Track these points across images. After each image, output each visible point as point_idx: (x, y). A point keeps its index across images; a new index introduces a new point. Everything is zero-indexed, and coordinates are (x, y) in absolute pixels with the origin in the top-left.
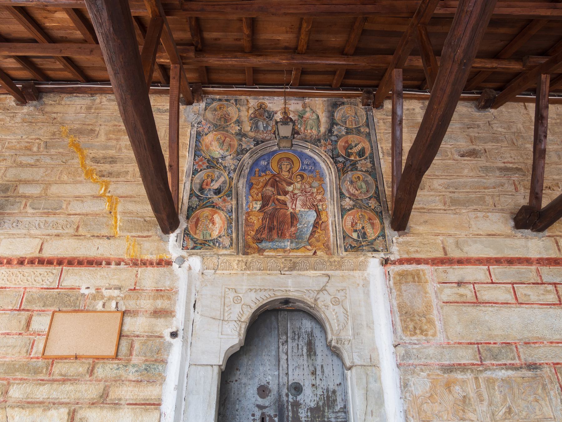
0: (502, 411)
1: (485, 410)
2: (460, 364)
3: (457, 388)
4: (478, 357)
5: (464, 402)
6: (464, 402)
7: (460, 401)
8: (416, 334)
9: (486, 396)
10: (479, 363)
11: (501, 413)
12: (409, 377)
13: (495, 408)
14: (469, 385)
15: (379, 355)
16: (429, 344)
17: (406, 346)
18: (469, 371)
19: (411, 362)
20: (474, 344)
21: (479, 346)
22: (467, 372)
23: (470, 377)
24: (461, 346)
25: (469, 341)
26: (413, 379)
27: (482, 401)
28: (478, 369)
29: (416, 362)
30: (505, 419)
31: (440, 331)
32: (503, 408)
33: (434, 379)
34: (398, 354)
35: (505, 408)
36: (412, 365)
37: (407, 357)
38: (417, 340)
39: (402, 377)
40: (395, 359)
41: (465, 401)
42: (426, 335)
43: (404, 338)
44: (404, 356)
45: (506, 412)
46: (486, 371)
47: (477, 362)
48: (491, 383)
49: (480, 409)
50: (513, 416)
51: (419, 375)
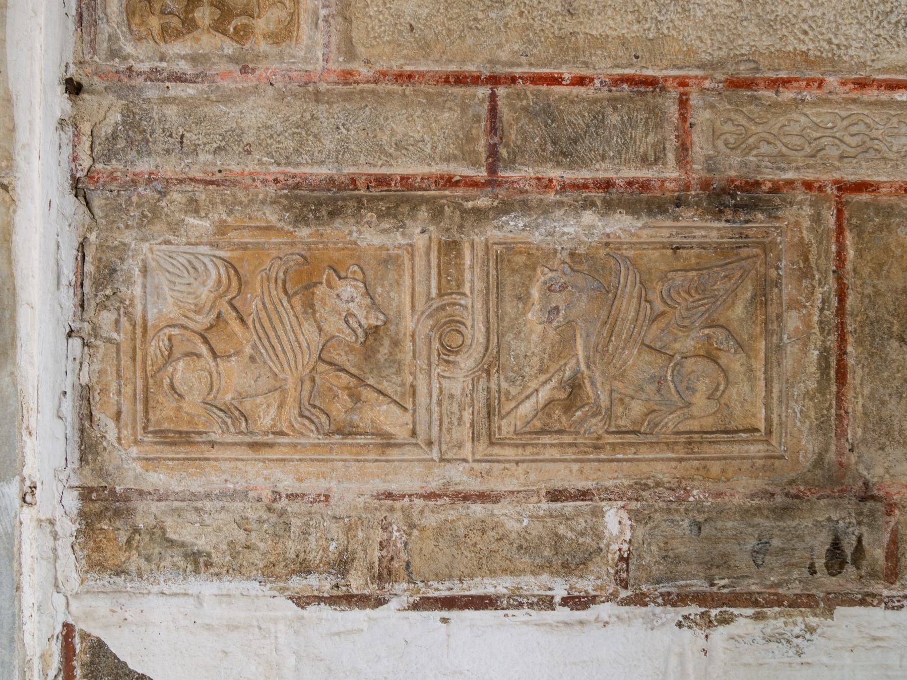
0: (533, 399)
1: (457, 392)
2: (383, 181)
3: (347, 289)
4: (481, 146)
5: (368, 351)
6: (368, 351)
7: (351, 349)
8: (190, 25)
9: (475, 332)
10: (482, 174)
11: (527, 408)
12: (128, 237)
13: (504, 385)
14: (407, 281)
15: (12, 130)
16: (251, 81)
17: (133, 88)
18: (423, 213)
19: (144, 166)
20: (476, 80)
21: (501, 91)
22: (413, 218)
23: (421, 241)
24: (409, 90)
25: (453, 68)
26: (145, 246)
27: (449, 352)
28: (470, 205)
29: (170, 167)
30: (542, 432)
31: (315, 13)
32: (544, 383)
33: (244, 247)
34: (86, 128)
35: (554, 382)
36: (149, 181)
37: (131, 142)
38: (194, 59)
39: (93, 237)
40: (67, 151)
41: (375, 351)
42: (242, 35)
43: (129, 49)
44: (114, 137)
45: (550, 403)
46: (507, 213)
47: (470, 172)
48: (513, 271)
49: (435, 386)
50: (582, 421)
51: (174, 227)
